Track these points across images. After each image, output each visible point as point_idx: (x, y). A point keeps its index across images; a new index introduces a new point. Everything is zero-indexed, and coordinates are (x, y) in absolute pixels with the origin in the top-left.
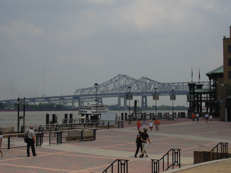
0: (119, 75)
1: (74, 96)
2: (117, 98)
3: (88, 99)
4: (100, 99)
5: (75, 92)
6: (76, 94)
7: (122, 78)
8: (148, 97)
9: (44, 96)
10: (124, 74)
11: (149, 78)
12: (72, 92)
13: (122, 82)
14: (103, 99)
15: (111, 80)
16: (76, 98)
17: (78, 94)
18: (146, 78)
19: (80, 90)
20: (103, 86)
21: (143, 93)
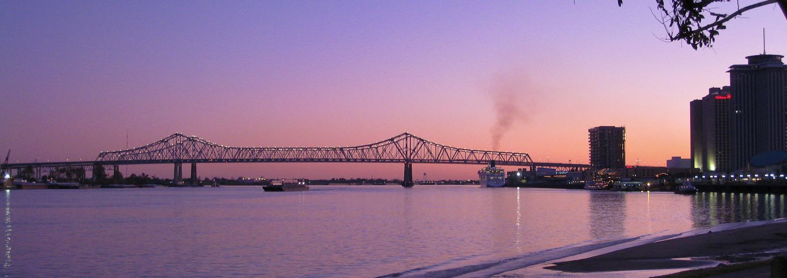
8: (198, 164)
9: (37, 162)
15: (162, 141)
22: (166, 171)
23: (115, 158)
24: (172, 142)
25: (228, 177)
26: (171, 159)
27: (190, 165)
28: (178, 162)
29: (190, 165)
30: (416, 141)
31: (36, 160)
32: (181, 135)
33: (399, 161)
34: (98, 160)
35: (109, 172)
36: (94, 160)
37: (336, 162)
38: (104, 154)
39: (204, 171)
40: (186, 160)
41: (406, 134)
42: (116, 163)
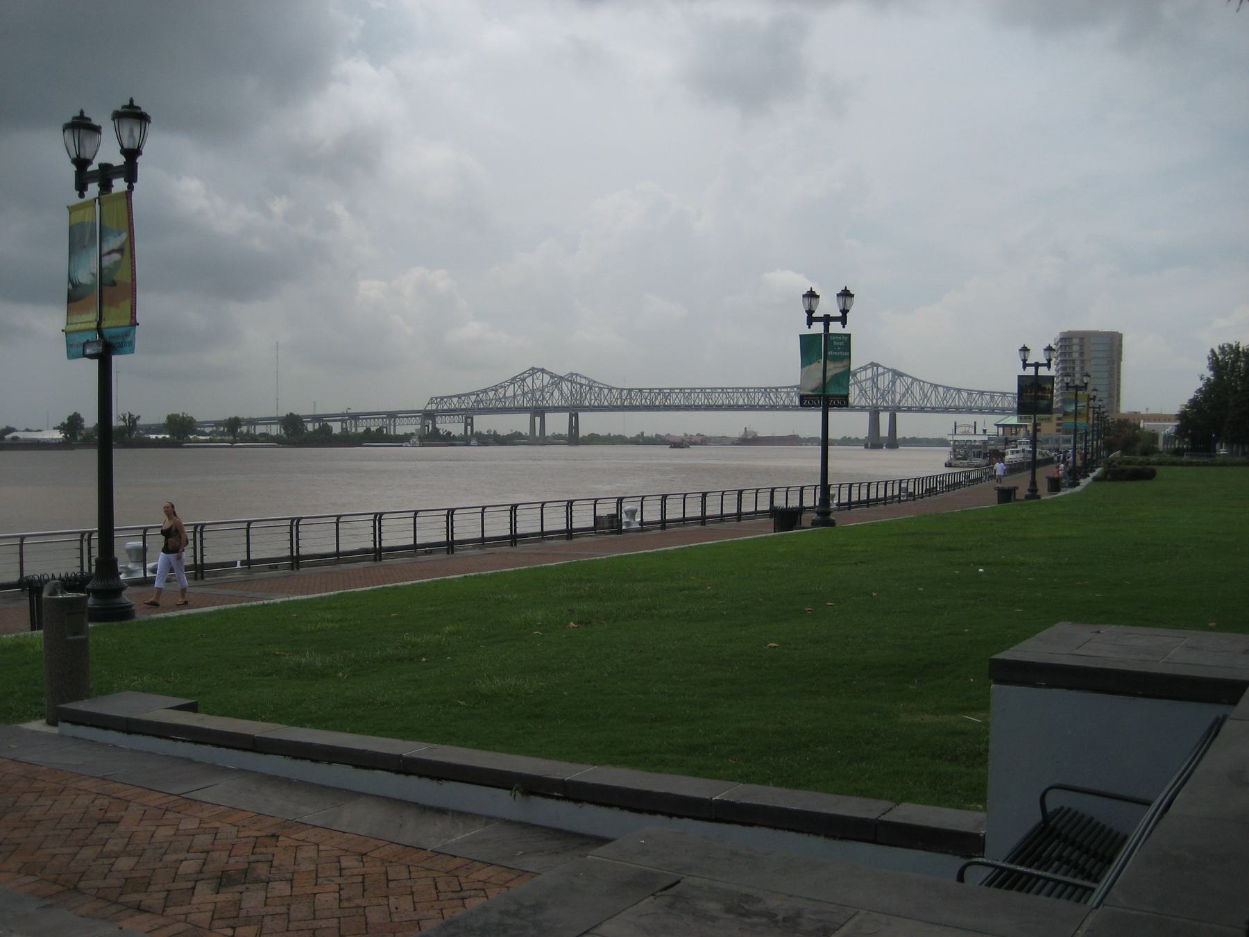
0: (533, 369)
1: (425, 410)
2: (528, 416)
3: (364, 421)
4: (469, 417)
5: (429, 404)
6: (429, 408)
7: (538, 374)
8: (581, 415)
9: (349, 411)
10: (541, 367)
11: (585, 376)
12: (421, 404)
13: (539, 381)
14: (475, 418)
15: (514, 378)
16: (429, 415)
17: (434, 407)
18: (577, 375)
19: (436, 398)
20: (493, 390)
21: (466, 410)
22: (521, 423)
23: (469, 403)
24: (529, 380)
25: (603, 432)
26: (760, 403)
27: (566, 415)
28: (539, 412)
29: (566, 415)
30: (888, 377)
31: (349, 409)
32: (543, 371)
33: (863, 409)
34: (427, 408)
35: (336, 428)
36: (422, 408)
37: (960, 412)
38: (438, 400)
39: (589, 423)
40: (765, 406)
41: (873, 365)
42: (468, 415)
